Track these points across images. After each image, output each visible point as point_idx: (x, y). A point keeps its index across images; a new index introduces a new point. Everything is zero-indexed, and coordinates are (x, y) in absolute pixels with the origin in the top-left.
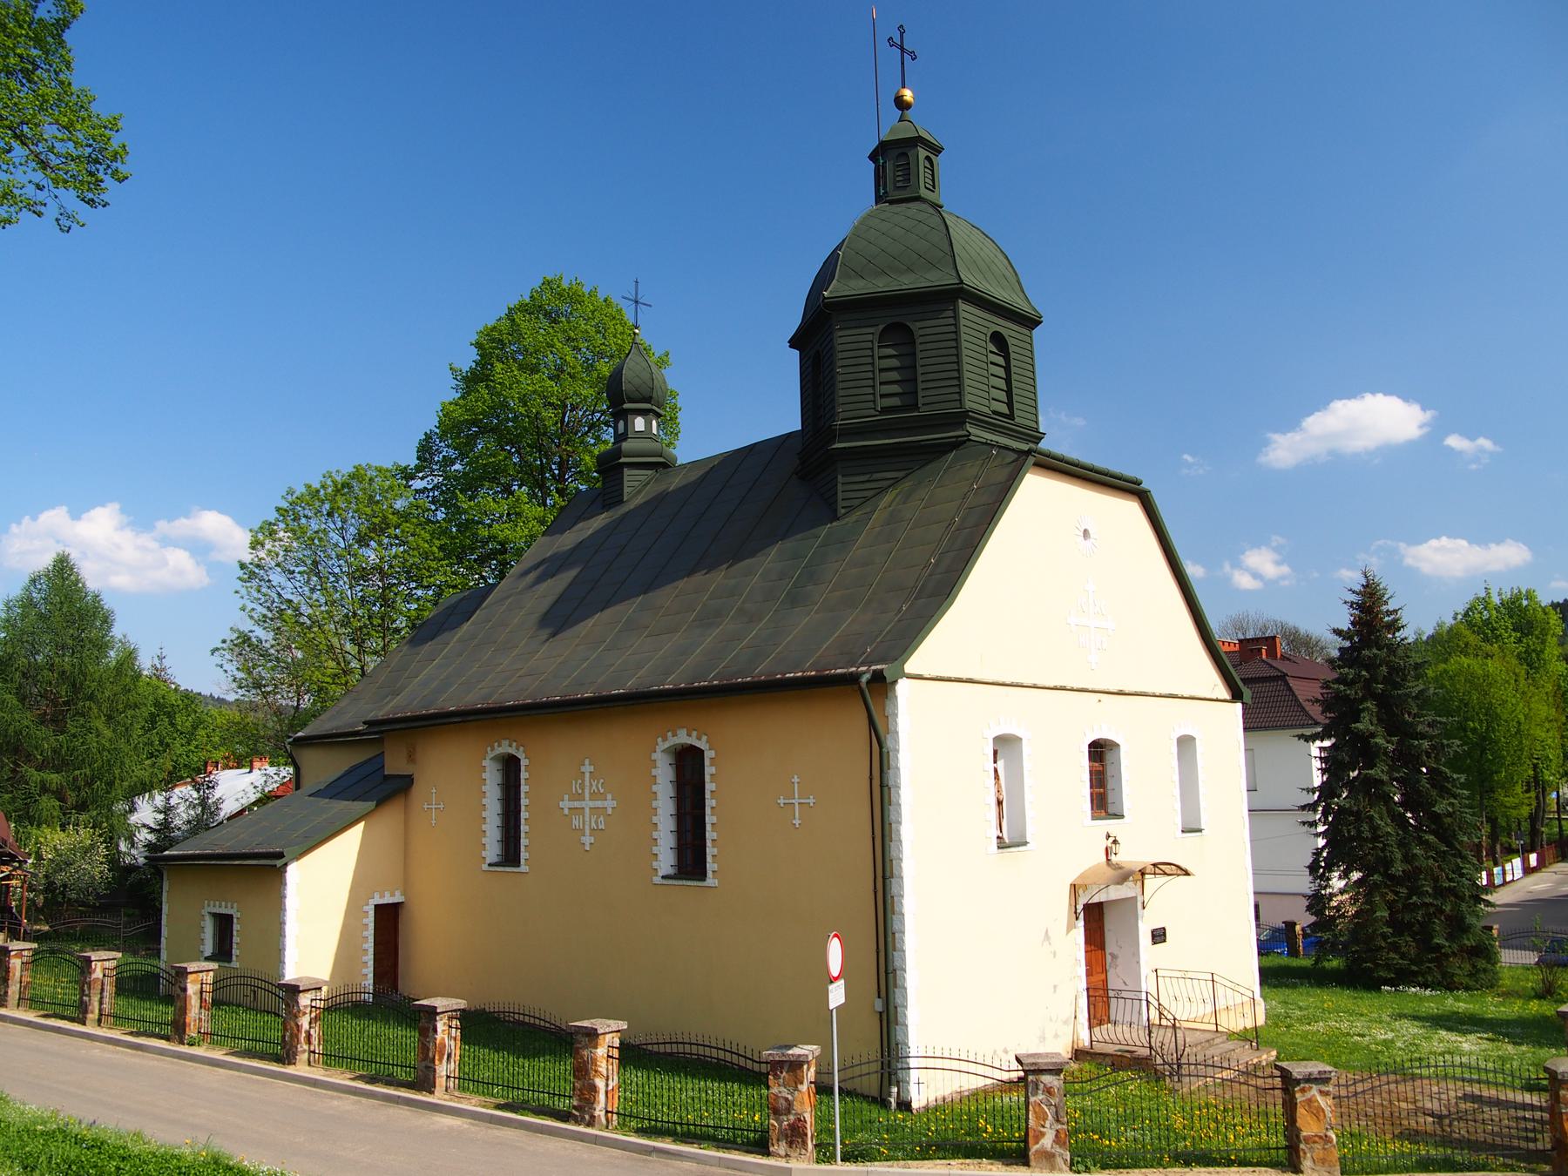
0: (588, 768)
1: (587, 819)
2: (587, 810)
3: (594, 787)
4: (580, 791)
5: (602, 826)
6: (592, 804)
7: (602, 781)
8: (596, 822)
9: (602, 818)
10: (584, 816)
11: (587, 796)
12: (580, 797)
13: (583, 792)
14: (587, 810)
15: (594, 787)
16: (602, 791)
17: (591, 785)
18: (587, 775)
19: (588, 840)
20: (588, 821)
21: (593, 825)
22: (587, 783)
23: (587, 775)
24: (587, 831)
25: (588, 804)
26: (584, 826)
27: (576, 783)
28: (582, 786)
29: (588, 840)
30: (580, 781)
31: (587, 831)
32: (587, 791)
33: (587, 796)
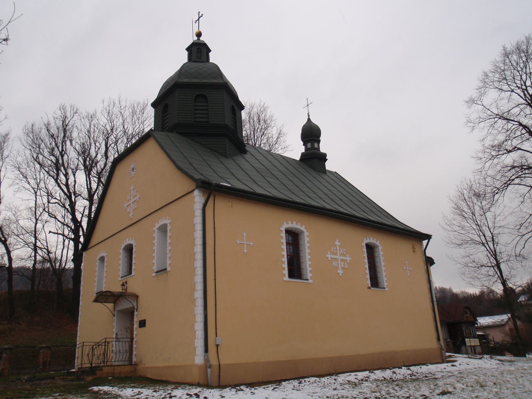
0: (337, 243)
1: (339, 263)
3: (341, 252)
5: (346, 267)
8: (344, 265)
9: (346, 264)
10: (338, 262)
11: (339, 254)
12: (336, 254)
13: (337, 252)
15: (341, 252)
16: (345, 253)
18: (338, 246)
20: (341, 265)
21: (342, 266)
22: (338, 249)
24: (340, 269)
25: (338, 257)
26: (338, 266)
27: (333, 249)
28: (336, 250)
29: (340, 272)
31: (340, 269)
32: (338, 251)
33: (339, 254)
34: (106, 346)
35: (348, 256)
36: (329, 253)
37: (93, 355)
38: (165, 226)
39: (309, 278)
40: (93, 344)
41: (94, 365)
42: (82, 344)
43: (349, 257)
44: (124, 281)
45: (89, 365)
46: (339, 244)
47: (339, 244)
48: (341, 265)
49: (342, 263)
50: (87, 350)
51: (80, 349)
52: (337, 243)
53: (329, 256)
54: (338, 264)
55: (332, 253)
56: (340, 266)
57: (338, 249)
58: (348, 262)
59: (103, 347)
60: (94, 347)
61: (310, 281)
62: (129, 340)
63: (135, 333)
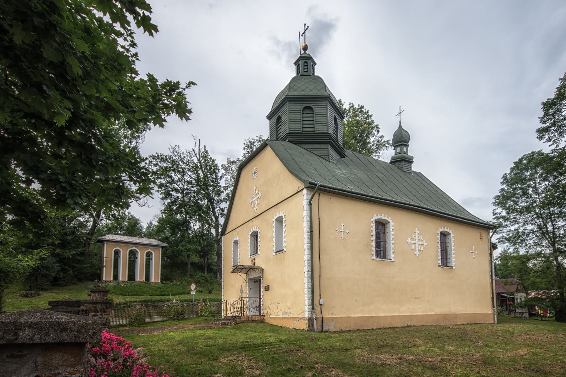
0: (417, 231)
1: (417, 247)
2: (417, 244)
4: (414, 238)
6: (419, 243)
7: (422, 237)
8: (421, 248)
9: (422, 247)
10: (416, 246)
11: (417, 240)
12: (415, 240)
14: (417, 244)
16: (422, 239)
17: (418, 237)
18: (417, 234)
19: (417, 253)
20: (418, 248)
21: (419, 249)
22: (417, 236)
23: (417, 234)
29: (417, 253)
30: (414, 235)
33: (417, 240)
34: (243, 303)
35: (424, 241)
36: (409, 239)
37: (233, 308)
38: (281, 217)
39: (392, 258)
40: (233, 301)
41: (234, 315)
42: (225, 301)
43: (425, 242)
44: (253, 258)
45: (231, 315)
46: (418, 232)
47: (418, 232)
48: (418, 248)
49: (419, 247)
50: (229, 305)
51: (225, 304)
52: (417, 231)
53: (409, 241)
54: (416, 247)
55: (411, 239)
56: (417, 249)
57: (417, 236)
58: (425, 246)
59: (240, 303)
60: (234, 303)
61: (393, 260)
62: (258, 299)
63: (262, 294)
